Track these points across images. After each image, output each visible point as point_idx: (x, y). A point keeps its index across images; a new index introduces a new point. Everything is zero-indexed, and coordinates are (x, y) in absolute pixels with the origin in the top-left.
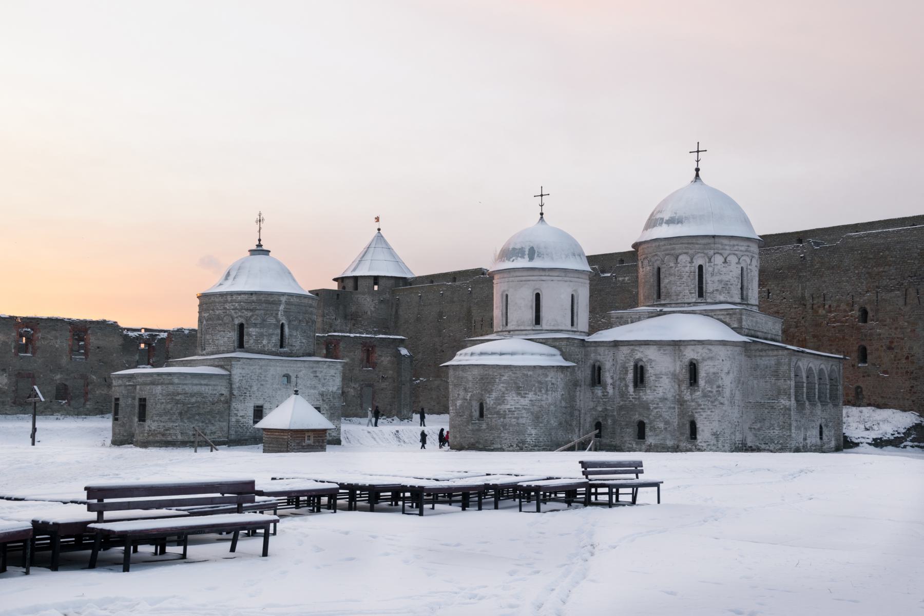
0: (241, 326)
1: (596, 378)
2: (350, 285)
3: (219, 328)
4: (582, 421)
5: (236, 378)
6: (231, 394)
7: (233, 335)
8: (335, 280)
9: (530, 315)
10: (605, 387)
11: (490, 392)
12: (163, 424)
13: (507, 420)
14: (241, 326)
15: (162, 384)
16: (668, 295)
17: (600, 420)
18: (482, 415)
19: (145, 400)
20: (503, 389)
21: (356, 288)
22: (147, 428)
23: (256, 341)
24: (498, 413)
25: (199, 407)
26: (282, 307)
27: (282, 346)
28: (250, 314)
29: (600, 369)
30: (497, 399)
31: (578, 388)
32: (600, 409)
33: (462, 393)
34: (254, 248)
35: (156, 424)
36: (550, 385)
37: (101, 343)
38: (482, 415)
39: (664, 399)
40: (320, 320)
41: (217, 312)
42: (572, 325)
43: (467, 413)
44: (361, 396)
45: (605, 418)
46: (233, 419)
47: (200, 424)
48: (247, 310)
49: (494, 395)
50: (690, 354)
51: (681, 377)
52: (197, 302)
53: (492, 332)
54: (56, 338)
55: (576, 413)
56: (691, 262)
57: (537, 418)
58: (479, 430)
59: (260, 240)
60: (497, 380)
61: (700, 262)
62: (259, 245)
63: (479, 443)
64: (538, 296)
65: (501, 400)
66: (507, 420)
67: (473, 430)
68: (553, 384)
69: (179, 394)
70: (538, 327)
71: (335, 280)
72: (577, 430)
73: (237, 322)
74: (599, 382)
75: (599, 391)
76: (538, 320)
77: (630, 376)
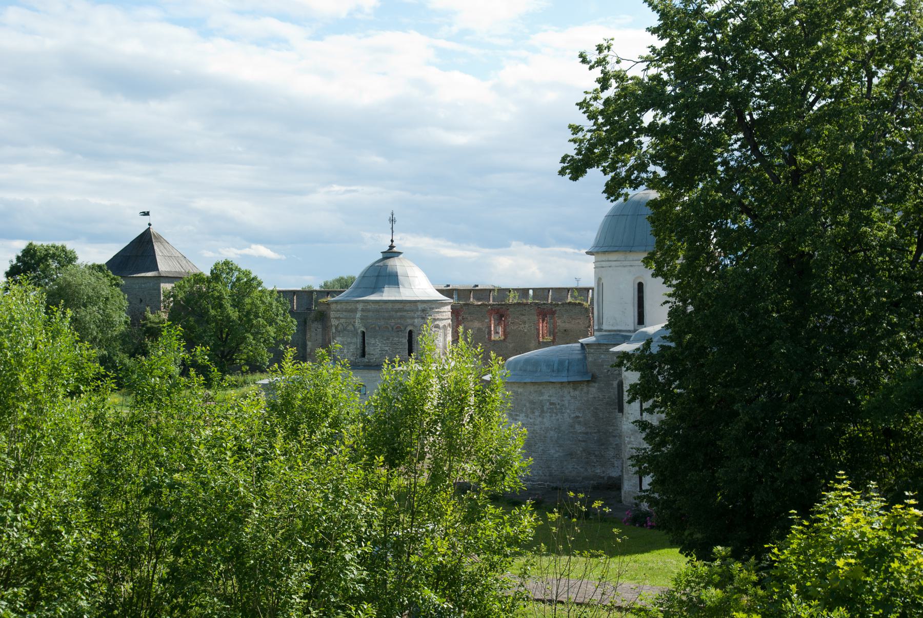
26: (359, 315)
37: (567, 326)
54: (525, 323)
59: (392, 241)
62: (392, 247)
68: (551, 404)
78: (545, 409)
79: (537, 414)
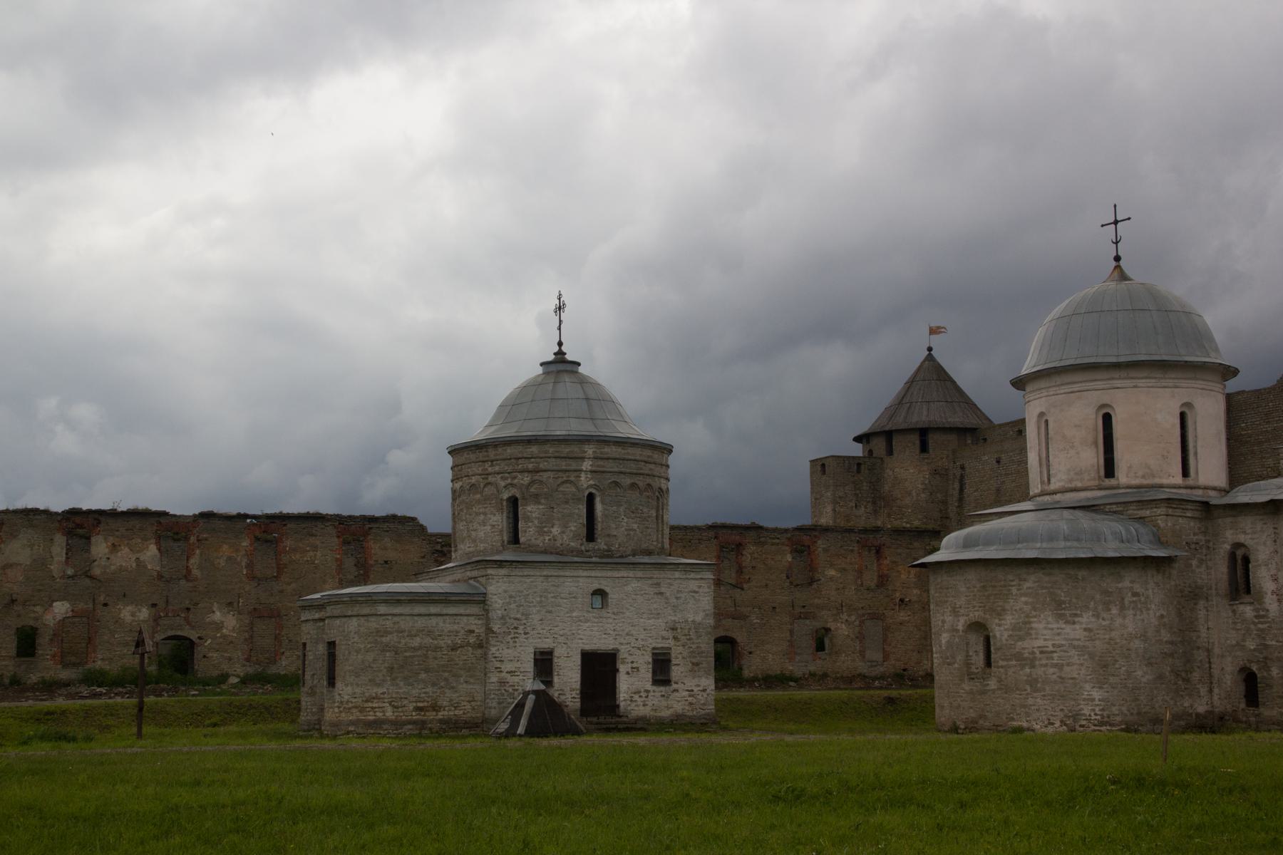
1: (1241, 581)
4: (1216, 672)
5: (497, 604)
6: (489, 630)
7: (499, 520)
8: (858, 439)
9: (1091, 458)
10: (1259, 599)
11: (1000, 614)
12: (358, 690)
13: (1039, 671)
14: (514, 502)
17: (1254, 668)
18: (988, 663)
19: (334, 643)
20: (1027, 608)
22: (337, 698)
23: (541, 532)
24: (1019, 657)
25: (426, 656)
27: (591, 537)
28: (526, 479)
29: (1246, 560)
30: (1015, 628)
31: (1202, 603)
32: (1251, 644)
33: (949, 619)
34: (551, 357)
36: (1128, 598)
38: (988, 663)
40: (829, 509)
41: (474, 480)
42: (1185, 473)
43: (960, 658)
44: (861, 637)
45: (1265, 663)
46: (494, 678)
47: (429, 689)
49: (1009, 619)
52: (449, 461)
53: (1026, 497)
55: (1200, 655)
57: (1103, 667)
58: (983, 693)
59: (560, 344)
60: (1014, 591)
62: (560, 353)
63: (985, 717)
64: (1107, 419)
65: (1022, 630)
66: (1039, 671)
67: (971, 692)
68: (1135, 594)
69: (387, 633)
70: (1109, 482)
71: (858, 439)
72: (1203, 691)
73: (505, 496)
74: (1248, 591)
75: (1248, 611)
76: (1110, 469)
78: (1126, 602)
79: (1114, 611)
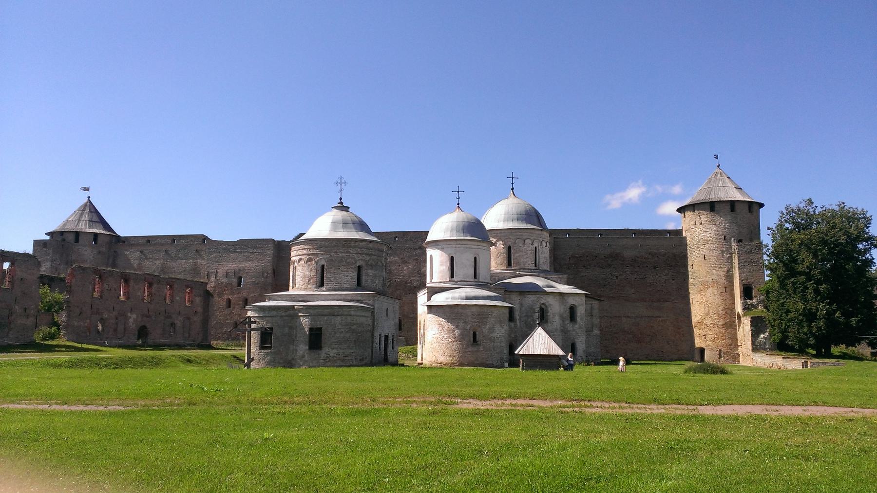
0: (359, 268)
2: (71, 238)
3: (342, 268)
12: (342, 351)
15: (342, 315)
16: (518, 264)
21: (77, 240)
24: (490, 339)
28: (368, 258)
30: (490, 329)
35: (335, 351)
39: (556, 330)
48: (366, 254)
50: (571, 301)
51: (565, 316)
56: (532, 244)
58: (477, 351)
61: (536, 245)
65: (492, 330)
75: (512, 324)
77: (537, 315)
